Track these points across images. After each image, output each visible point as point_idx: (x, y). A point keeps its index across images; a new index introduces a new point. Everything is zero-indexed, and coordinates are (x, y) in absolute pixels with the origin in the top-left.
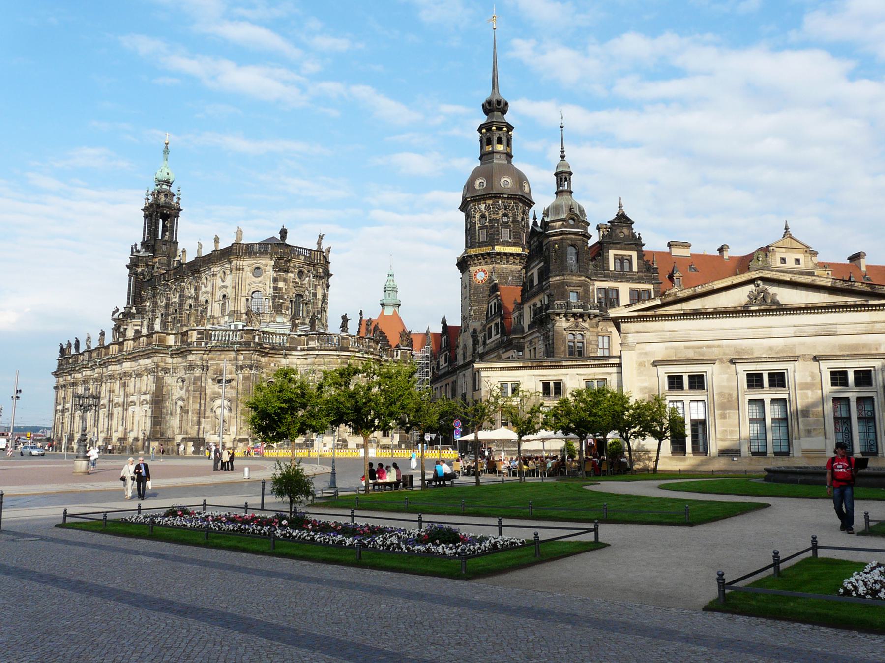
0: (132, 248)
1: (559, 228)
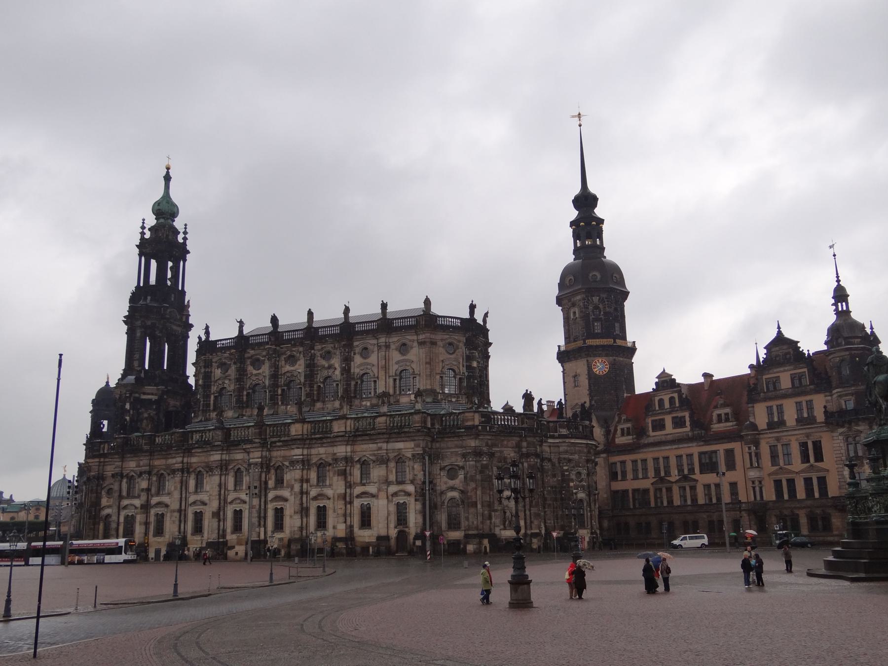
1: (857, 344)
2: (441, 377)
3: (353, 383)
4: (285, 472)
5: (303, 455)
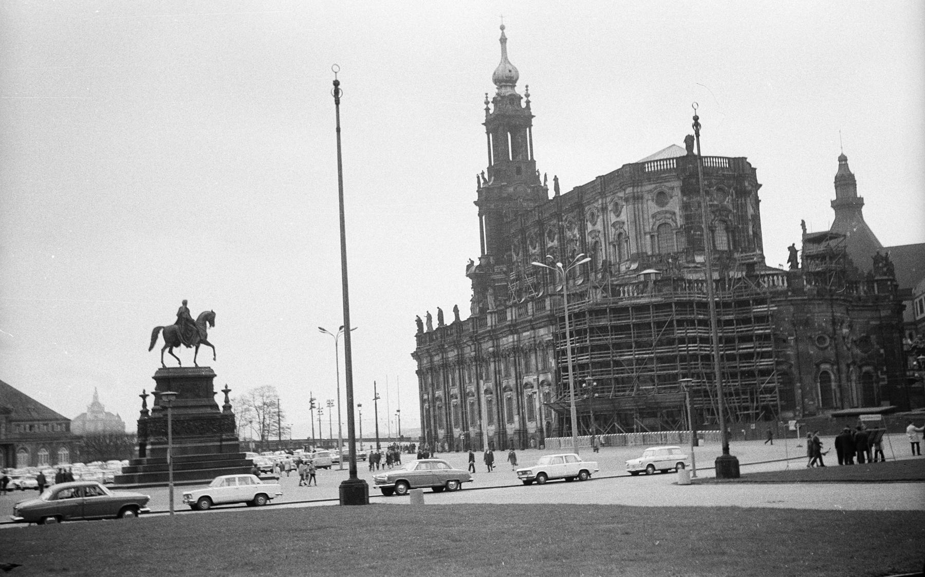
0: (478, 177)
2: (652, 237)
5: (493, 347)
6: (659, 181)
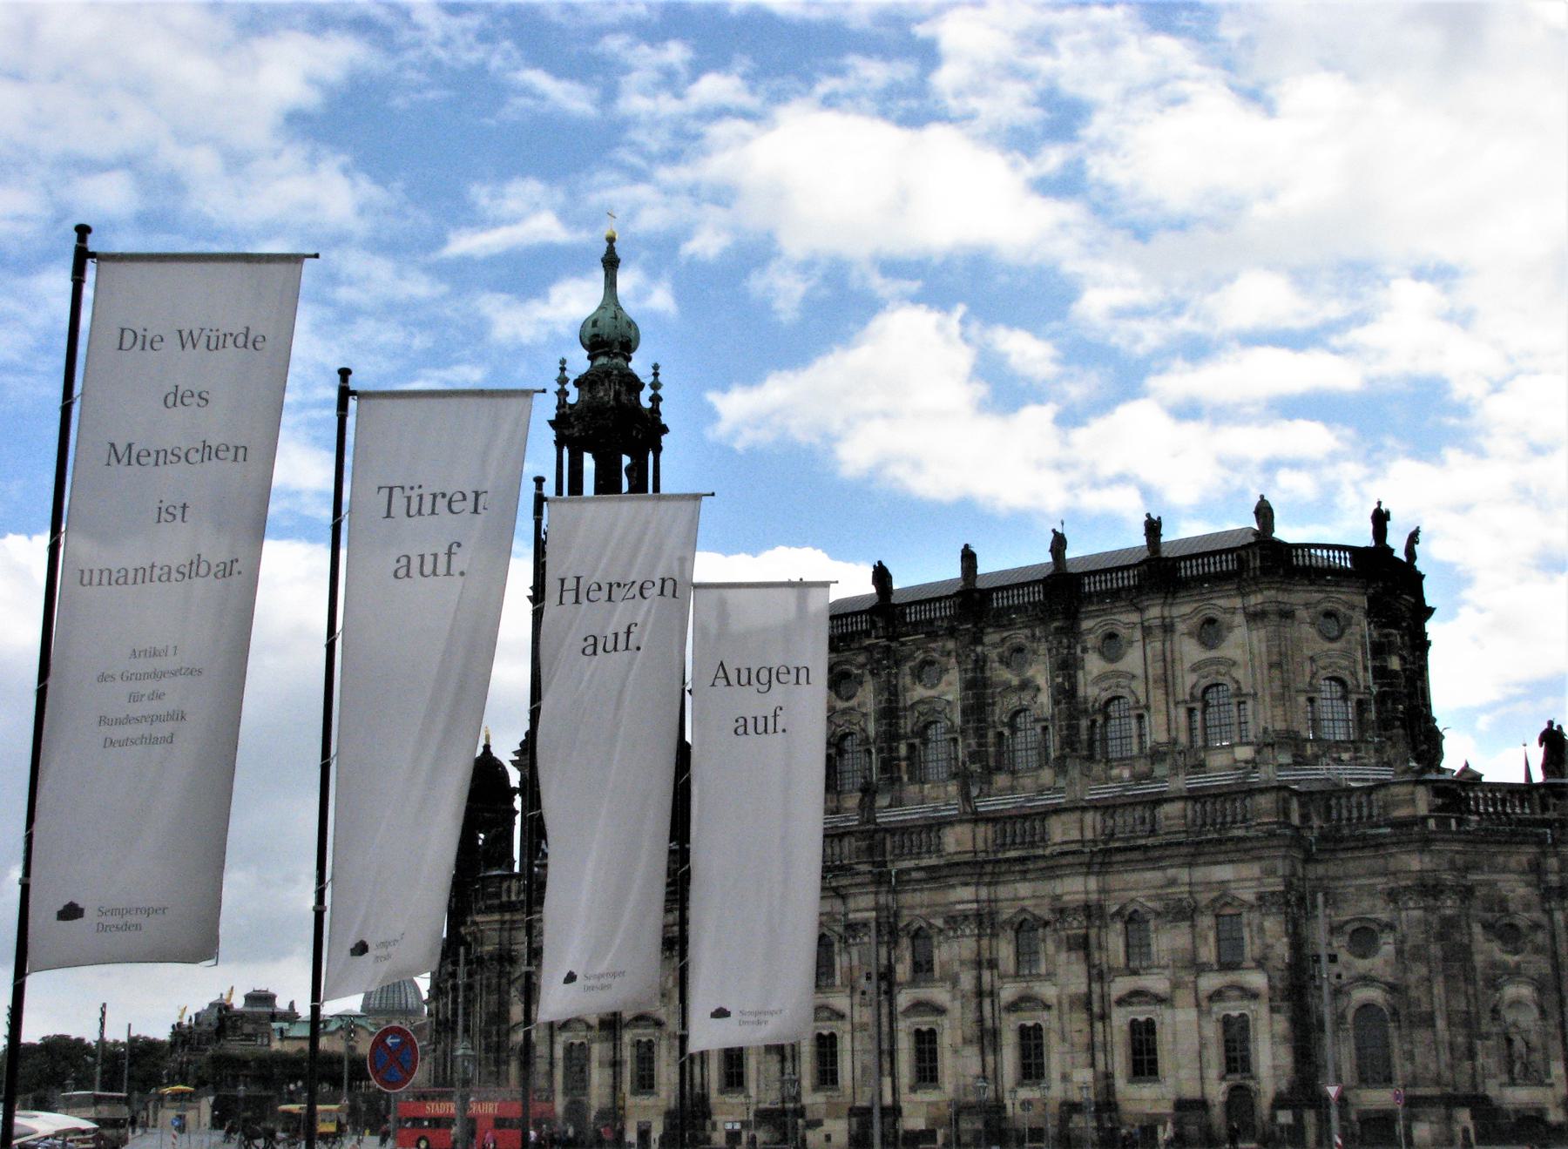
2: (1311, 700)
3: (1084, 723)
4: (936, 943)
5: (977, 901)
6: (1328, 589)
